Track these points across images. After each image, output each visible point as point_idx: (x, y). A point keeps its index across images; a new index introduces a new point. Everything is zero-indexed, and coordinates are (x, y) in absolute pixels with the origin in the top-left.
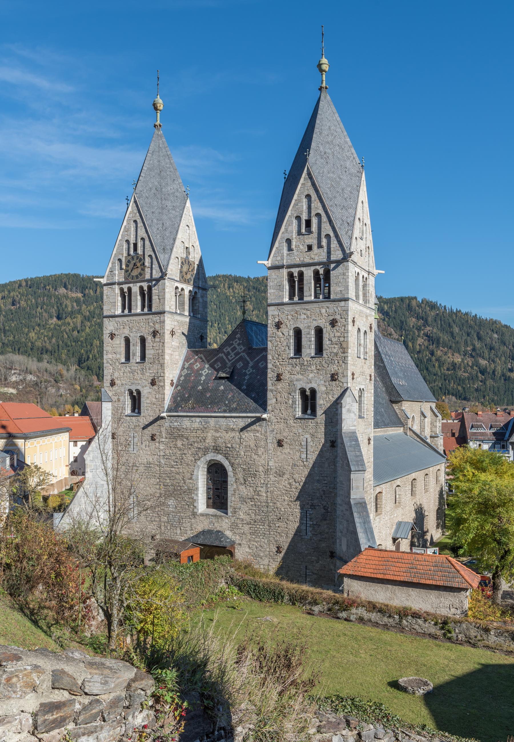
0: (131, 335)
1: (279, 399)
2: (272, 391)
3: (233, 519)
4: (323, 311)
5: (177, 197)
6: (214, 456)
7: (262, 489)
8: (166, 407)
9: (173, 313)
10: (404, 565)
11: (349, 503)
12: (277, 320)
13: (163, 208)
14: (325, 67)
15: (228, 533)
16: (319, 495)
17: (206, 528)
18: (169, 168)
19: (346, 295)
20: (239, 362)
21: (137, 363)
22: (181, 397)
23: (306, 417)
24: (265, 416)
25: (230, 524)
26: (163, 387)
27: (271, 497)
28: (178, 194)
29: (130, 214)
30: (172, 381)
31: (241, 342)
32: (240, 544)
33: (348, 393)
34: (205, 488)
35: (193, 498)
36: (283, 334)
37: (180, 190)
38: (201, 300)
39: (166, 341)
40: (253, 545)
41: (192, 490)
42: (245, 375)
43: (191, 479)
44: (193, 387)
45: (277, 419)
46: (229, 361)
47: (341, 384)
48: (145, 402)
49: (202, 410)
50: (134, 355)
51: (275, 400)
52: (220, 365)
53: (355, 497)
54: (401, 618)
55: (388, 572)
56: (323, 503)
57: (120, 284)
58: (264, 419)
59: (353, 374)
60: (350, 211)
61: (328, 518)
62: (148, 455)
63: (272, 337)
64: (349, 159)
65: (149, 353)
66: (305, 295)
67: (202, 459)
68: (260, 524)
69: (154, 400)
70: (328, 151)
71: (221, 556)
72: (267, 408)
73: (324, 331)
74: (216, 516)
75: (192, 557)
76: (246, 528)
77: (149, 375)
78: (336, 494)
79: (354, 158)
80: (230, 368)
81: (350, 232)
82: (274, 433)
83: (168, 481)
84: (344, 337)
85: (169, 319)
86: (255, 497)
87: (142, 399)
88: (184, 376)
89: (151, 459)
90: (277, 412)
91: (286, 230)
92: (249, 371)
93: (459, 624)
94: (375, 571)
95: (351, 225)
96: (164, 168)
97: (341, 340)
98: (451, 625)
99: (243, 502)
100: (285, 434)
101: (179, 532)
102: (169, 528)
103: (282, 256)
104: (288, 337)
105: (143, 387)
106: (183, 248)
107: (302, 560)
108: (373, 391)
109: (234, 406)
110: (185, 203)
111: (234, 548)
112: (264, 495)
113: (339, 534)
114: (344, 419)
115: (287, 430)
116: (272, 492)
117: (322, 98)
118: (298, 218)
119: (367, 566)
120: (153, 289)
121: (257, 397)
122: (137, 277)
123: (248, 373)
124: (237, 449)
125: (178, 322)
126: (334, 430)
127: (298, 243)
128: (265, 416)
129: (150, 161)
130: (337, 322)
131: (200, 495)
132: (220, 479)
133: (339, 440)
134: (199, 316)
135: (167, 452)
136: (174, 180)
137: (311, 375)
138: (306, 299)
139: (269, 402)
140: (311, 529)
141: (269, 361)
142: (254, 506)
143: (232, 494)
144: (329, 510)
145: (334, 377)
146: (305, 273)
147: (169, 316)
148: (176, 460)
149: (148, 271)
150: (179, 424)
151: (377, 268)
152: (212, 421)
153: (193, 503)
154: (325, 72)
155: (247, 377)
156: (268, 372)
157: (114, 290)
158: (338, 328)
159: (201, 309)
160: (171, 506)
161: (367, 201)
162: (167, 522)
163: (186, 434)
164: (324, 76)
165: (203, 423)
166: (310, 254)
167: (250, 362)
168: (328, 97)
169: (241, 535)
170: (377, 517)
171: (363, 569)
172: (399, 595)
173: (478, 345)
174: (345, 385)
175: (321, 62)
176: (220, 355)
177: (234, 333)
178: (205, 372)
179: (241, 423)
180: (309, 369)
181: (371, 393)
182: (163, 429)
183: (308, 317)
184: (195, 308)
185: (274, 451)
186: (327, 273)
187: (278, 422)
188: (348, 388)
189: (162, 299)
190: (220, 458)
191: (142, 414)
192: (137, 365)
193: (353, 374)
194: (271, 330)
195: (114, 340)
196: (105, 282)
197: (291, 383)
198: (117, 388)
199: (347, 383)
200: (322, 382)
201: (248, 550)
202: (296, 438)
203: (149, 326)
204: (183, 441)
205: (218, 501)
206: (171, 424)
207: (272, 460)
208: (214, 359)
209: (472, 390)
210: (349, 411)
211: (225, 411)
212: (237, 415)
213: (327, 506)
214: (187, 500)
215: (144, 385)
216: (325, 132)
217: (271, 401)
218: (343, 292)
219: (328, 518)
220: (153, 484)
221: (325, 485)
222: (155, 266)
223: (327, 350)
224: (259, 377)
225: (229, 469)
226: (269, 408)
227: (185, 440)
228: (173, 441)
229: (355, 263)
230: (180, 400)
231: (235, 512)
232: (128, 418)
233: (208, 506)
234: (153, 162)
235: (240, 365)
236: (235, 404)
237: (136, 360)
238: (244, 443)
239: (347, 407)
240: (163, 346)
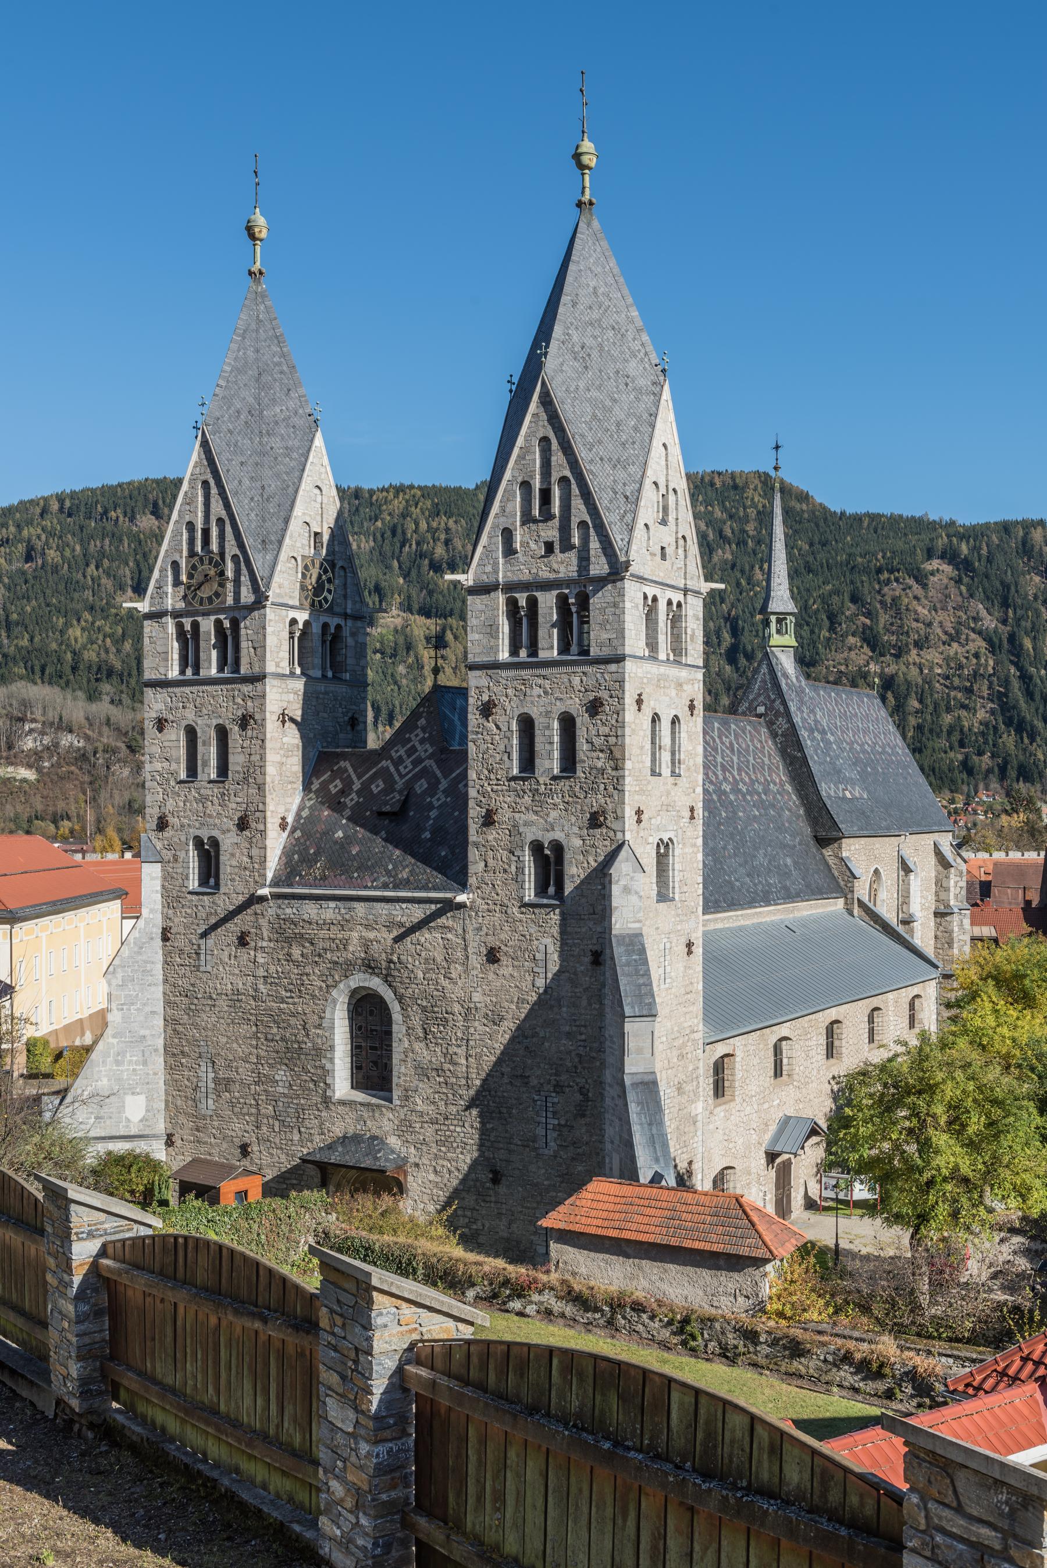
0: (199, 722)
1: (491, 862)
2: (476, 845)
3: (402, 1112)
4: (576, 681)
5: (294, 427)
6: (365, 980)
7: (458, 1051)
8: (270, 875)
9: (284, 675)
10: (658, 1213)
11: (622, 1084)
12: (485, 698)
13: (263, 454)
14: (588, 160)
15: (393, 1141)
16: (570, 1065)
17: (351, 1131)
18: (279, 364)
19: (619, 648)
20: (421, 778)
21: (210, 782)
22: (300, 853)
23: (545, 901)
24: (462, 898)
25: (396, 1122)
26: (263, 832)
27: (477, 1068)
28: (296, 421)
29: (195, 467)
30: (283, 819)
31: (427, 735)
32: (417, 1165)
33: (624, 853)
34: (349, 1047)
35: (323, 1068)
36: (498, 727)
37: (301, 411)
38: (350, 641)
39: (268, 736)
40: (443, 1166)
41: (322, 1052)
42: (431, 806)
43: (319, 1026)
44: (325, 833)
45: (488, 904)
46: (401, 776)
47: (611, 834)
48: (228, 863)
49: (341, 883)
50: (206, 764)
51: (483, 864)
52: (382, 785)
53: (634, 1070)
54: (613, 1311)
55: (629, 1225)
56: (578, 1080)
57: (176, 615)
58: (461, 906)
59: (639, 812)
60: (632, 469)
61: (588, 1113)
62: (234, 975)
63: (477, 733)
64: (635, 356)
65: (236, 760)
66: (540, 646)
67: (341, 986)
68: (455, 1122)
69: (245, 859)
70: (589, 342)
71: (306, 1193)
72: (467, 880)
73: (578, 721)
74: (368, 1105)
75: (246, 1192)
76: (429, 1131)
77: (235, 808)
78: (603, 1064)
79: (646, 354)
80: (400, 792)
81: (629, 518)
82: (483, 933)
83: (275, 1030)
84: (617, 737)
85: (275, 690)
86: (446, 1066)
87: (221, 858)
88: (310, 808)
89: (241, 986)
90: (487, 889)
91: (503, 509)
92: (438, 799)
93: (709, 1324)
94: (606, 1224)
95: (633, 500)
96: (268, 365)
97: (610, 743)
98: (694, 1327)
99: (422, 1078)
100: (503, 936)
101: (296, 1137)
102: (277, 1129)
103: (496, 564)
104: (508, 734)
105: (224, 832)
106: (307, 535)
107: (539, 1198)
108: (700, 842)
109: (405, 874)
110: (312, 441)
111: (405, 1173)
112: (464, 1062)
113: (608, 1146)
114: (617, 908)
115: (507, 928)
116: (478, 1057)
117: (582, 225)
118: (526, 486)
119: (593, 1213)
120: (242, 625)
123: (436, 804)
124: (410, 966)
125: (295, 693)
126: (599, 929)
127: (527, 538)
128: (462, 898)
129: (239, 351)
130: (602, 704)
131: (337, 1061)
132: (378, 1028)
133: (608, 951)
134: (347, 676)
135: (272, 969)
136: (289, 390)
137: (554, 814)
138: (543, 655)
139: (472, 869)
140: (555, 1134)
141: (471, 783)
142: (444, 1085)
143: (401, 1060)
144: (590, 1095)
145: (595, 821)
146: (540, 600)
147: (276, 682)
148: (291, 987)
149: (230, 586)
150: (295, 911)
151: (708, 578)
152: (360, 908)
153: (323, 1078)
154: (590, 168)
155: (433, 814)
156: (470, 806)
157: (164, 627)
158: (604, 718)
159: (350, 661)
160: (280, 1084)
161: (677, 441)
162: (273, 1118)
163: (309, 931)
164: (587, 177)
165: (343, 911)
166: (549, 562)
168: (596, 224)
169: (419, 1146)
170: (719, 1109)
171: (584, 1220)
172: (647, 1269)
174: (619, 835)
175: (579, 151)
176: (384, 763)
177: (415, 715)
178: (352, 800)
179: (418, 913)
180: (550, 801)
181: (694, 845)
182: (263, 922)
183: (546, 693)
184: (339, 659)
185: (482, 972)
186: (584, 602)
187: (489, 911)
188: (623, 843)
189: (259, 648)
190: (376, 983)
191: (223, 890)
192: (211, 785)
193: (639, 812)
194: (474, 718)
195: (165, 731)
196: (147, 610)
197: (514, 830)
198: (171, 833)
199: (623, 832)
200: (576, 830)
201: (432, 1177)
202: (524, 945)
203: (234, 703)
204: (304, 947)
205: (375, 1073)
206: (279, 912)
207: (479, 989)
208: (371, 773)
210: (627, 890)
211: (385, 886)
212: (410, 894)
213: (587, 1086)
214: (312, 1071)
215: (225, 827)
216: (584, 301)
217: (476, 867)
218: (615, 643)
219: (588, 1113)
220: (245, 1037)
221: (582, 1043)
222: (245, 579)
223: (584, 761)
224: (456, 814)
225: (395, 1007)
226: (472, 881)
227: (307, 945)
228: (283, 948)
229: (641, 579)
230: (299, 860)
231: (407, 1098)
232: (194, 898)
233: (357, 1084)
234: (244, 354)
235: (421, 786)
236: (407, 870)
237: (209, 774)
238: (423, 954)
239: (622, 882)
240: (263, 747)
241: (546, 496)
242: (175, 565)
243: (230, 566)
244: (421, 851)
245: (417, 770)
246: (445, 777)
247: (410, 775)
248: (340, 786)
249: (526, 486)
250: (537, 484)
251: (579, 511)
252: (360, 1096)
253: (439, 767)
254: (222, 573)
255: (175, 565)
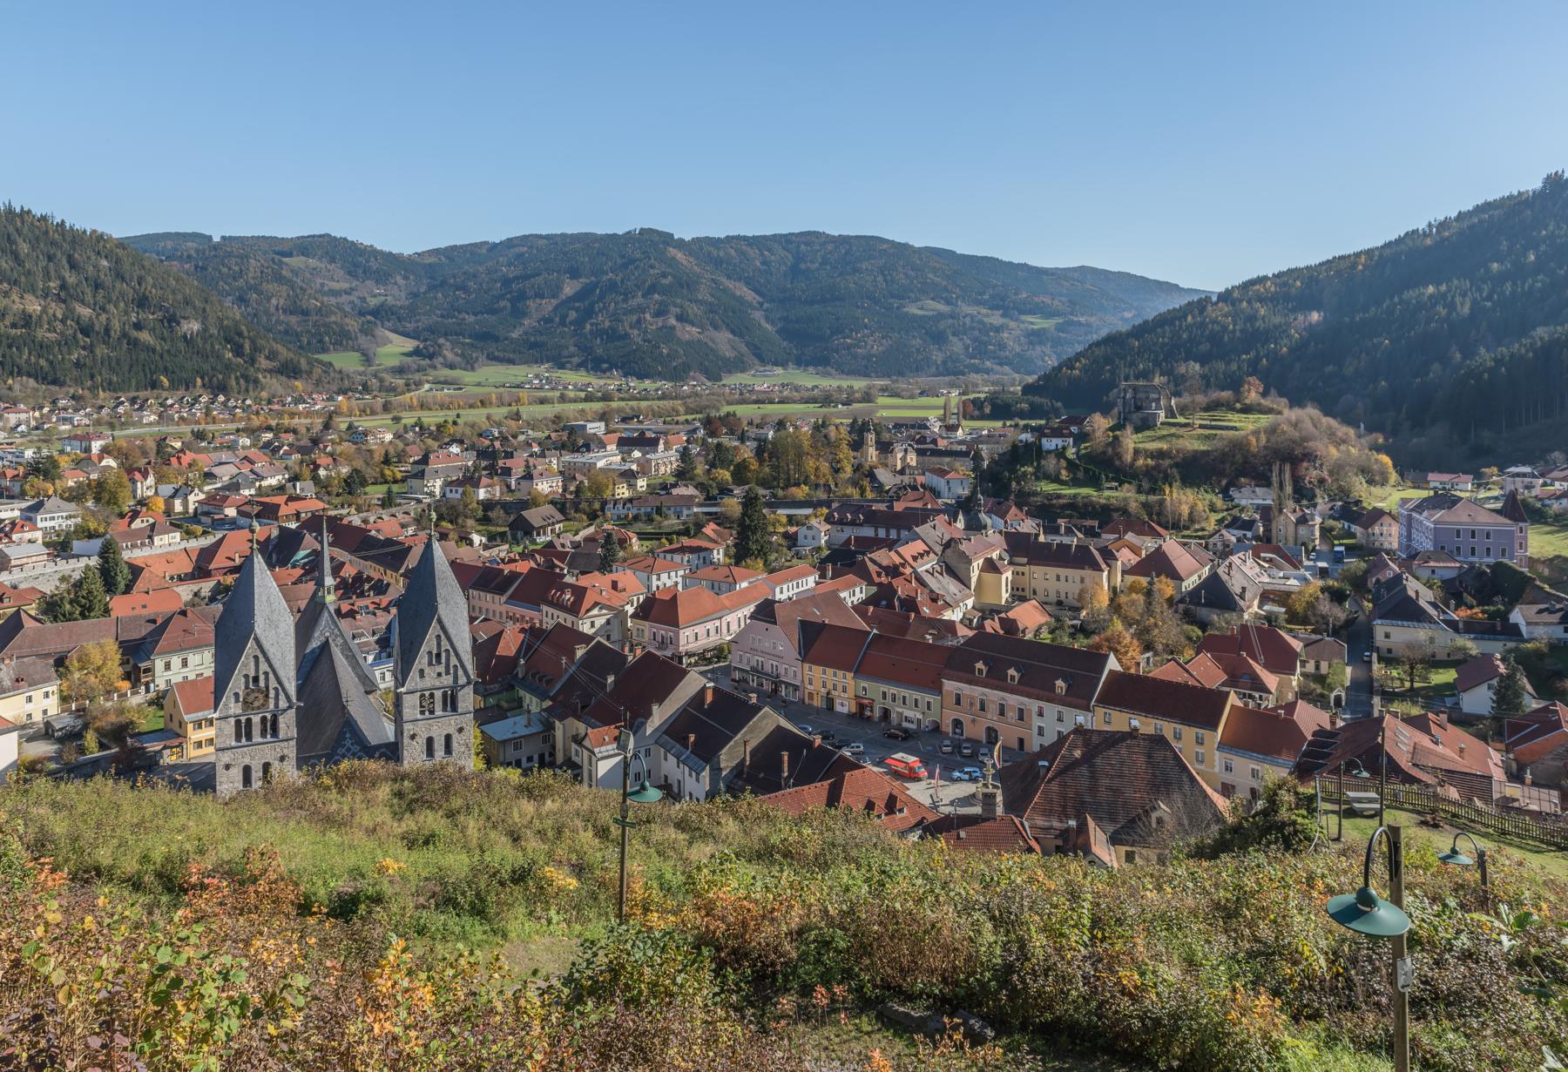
122: (259, 708)
173: (71, 279)
209: (68, 365)
241: (438, 656)
242: (236, 695)
243: (272, 694)
249: (430, 653)
250: (435, 652)
251: (454, 661)
254: (267, 696)
255: (236, 695)
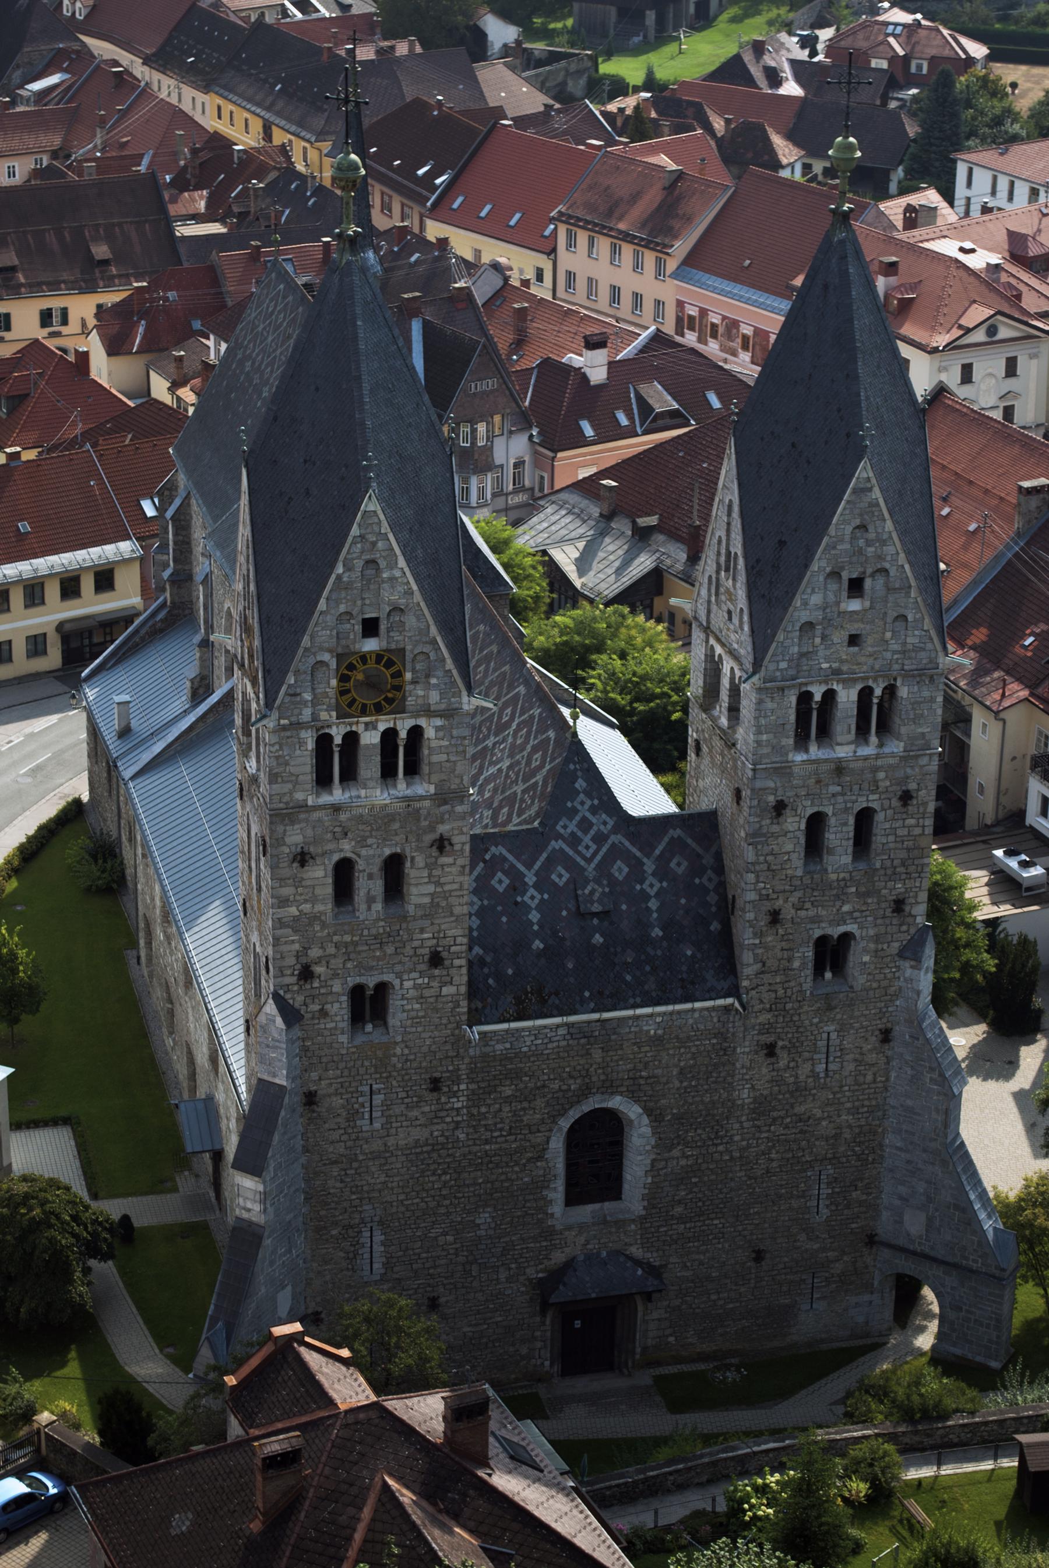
6: (604, 1100)
42: (645, 897)
67: (571, 1112)
121: (699, 956)
123: (652, 892)
167: (645, 860)
190: (616, 1102)
195: (306, 868)
244: (659, 953)
245: (604, 849)
246: (648, 856)
247: (599, 857)
248: (507, 881)
252: (586, 1212)
253: (633, 844)
